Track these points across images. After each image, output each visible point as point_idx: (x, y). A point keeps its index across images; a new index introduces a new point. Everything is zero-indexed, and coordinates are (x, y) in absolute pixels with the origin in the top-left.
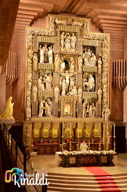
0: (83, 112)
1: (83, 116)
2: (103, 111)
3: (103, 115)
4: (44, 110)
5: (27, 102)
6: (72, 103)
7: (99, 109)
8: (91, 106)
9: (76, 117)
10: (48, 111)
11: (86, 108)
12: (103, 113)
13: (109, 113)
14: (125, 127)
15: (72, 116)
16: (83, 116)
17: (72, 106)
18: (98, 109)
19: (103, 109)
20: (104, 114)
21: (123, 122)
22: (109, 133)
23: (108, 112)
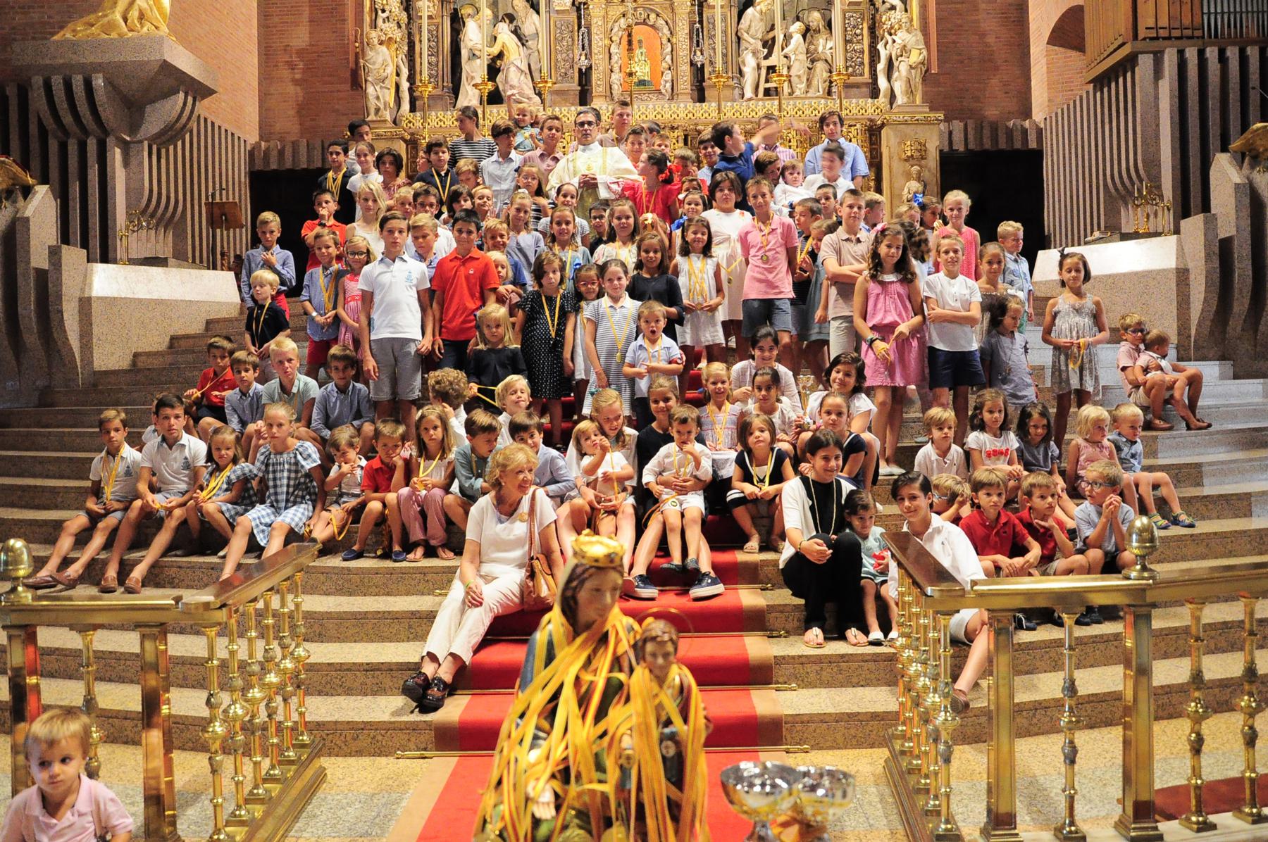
0: (745, 69)
1: (749, 93)
2: (884, 54)
3: (882, 82)
4: (493, 71)
5: (380, 21)
6: (666, 15)
7: (858, 47)
8: (798, 26)
9: (700, 95)
10: (513, 69)
11: (769, 45)
12: (881, 66)
13: (915, 57)
14: (1037, 156)
15: (672, 98)
16: (749, 93)
17: (666, 30)
18: (847, 42)
19: (880, 46)
20: (889, 78)
21: (1027, 124)
22: (914, 185)
23: (904, 50)
